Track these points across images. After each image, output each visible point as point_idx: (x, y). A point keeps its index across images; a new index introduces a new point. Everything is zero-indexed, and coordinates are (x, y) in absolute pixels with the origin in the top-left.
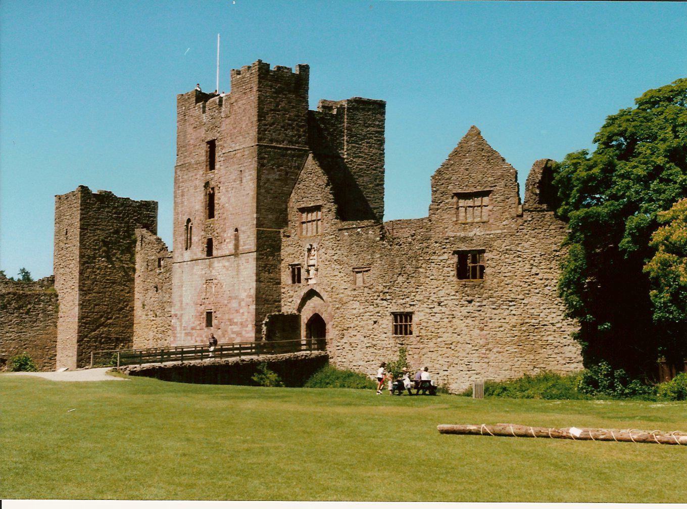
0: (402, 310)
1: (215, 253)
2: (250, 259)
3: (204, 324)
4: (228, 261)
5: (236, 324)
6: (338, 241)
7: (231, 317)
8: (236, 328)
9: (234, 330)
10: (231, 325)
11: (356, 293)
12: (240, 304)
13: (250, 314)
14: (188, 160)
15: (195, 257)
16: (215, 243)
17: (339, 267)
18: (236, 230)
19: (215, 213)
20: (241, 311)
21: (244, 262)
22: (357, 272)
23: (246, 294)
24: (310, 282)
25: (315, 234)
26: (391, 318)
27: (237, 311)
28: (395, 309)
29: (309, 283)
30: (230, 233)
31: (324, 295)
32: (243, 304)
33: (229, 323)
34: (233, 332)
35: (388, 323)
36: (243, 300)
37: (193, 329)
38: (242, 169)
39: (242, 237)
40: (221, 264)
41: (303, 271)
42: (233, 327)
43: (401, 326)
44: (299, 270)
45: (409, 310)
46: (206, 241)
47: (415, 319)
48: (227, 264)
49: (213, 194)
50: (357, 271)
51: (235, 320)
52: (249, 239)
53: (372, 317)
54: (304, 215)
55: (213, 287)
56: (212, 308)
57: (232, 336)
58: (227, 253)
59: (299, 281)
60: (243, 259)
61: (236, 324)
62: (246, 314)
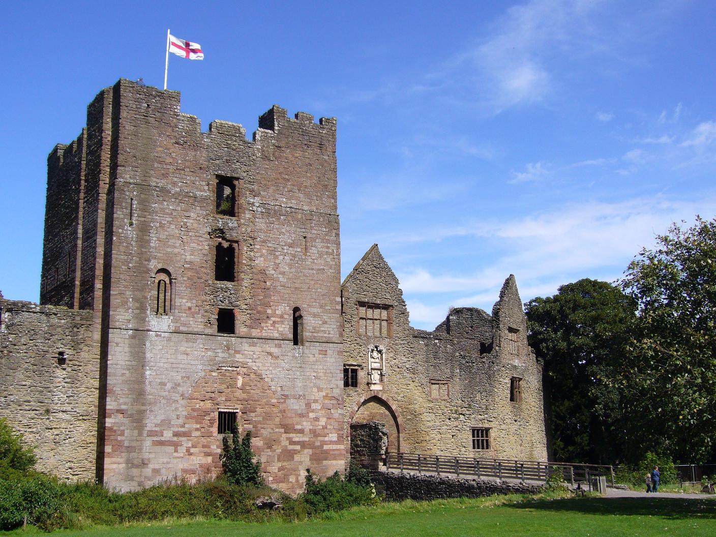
0: (481, 425)
1: (240, 329)
2: (329, 352)
3: (215, 429)
4: (280, 346)
5: (301, 431)
6: (411, 348)
7: (290, 421)
8: (296, 438)
9: (297, 439)
10: (285, 432)
11: (431, 405)
12: (308, 405)
13: (332, 421)
14: (153, 182)
15: (182, 329)
16: (241, 318)
17: (412, 376)
18: (296, 310)
19: (242, 276)
20: (312, 415)
21: (316, 351)
22: (432, 384)
23: (324, 394)
24: (373, 387)
25: (377, 334)
26: (470, 433)
27: (301, 416)
28: (474, 424)
29: (371, 389)
30: (284, 310)
31: (393, 404)
32: (314, 406)
33: (283, 430)
34: (292, 443)
35: (468, 437)
36: (316, 401)
37: (176, 434)
38: (309, 235)
39: (309, 322)
40: (257, 349)
41: (361, 374)
42: (291, 435)
43: (482, 440)
44: (355, 372)
45: (486, 425)
46: (217, 311)
47: (493, 434)
48: (275, 350)
49: (231, 250)
50: (433, 382)
51: (298, 427)
52: (326, 326)
53: (450, 431)
54: (362, 310)
55: (239, 377)
56: (238, 409)
57: (291, 447)
58: (276, 335)
59: (355, 384)
60: (310, 351)
61: (301, 431)
62: (323, 421)
